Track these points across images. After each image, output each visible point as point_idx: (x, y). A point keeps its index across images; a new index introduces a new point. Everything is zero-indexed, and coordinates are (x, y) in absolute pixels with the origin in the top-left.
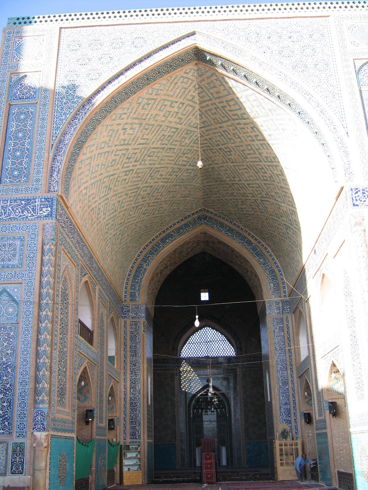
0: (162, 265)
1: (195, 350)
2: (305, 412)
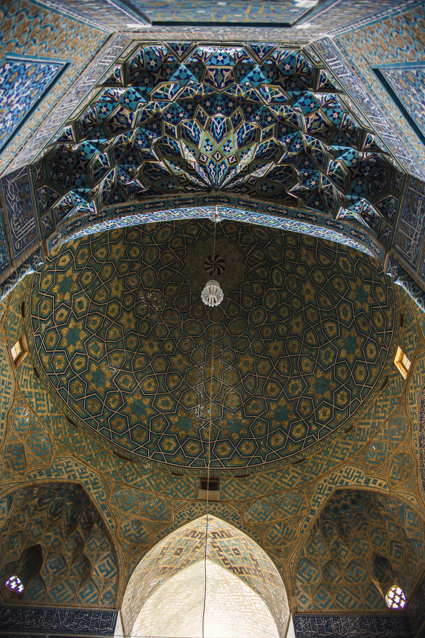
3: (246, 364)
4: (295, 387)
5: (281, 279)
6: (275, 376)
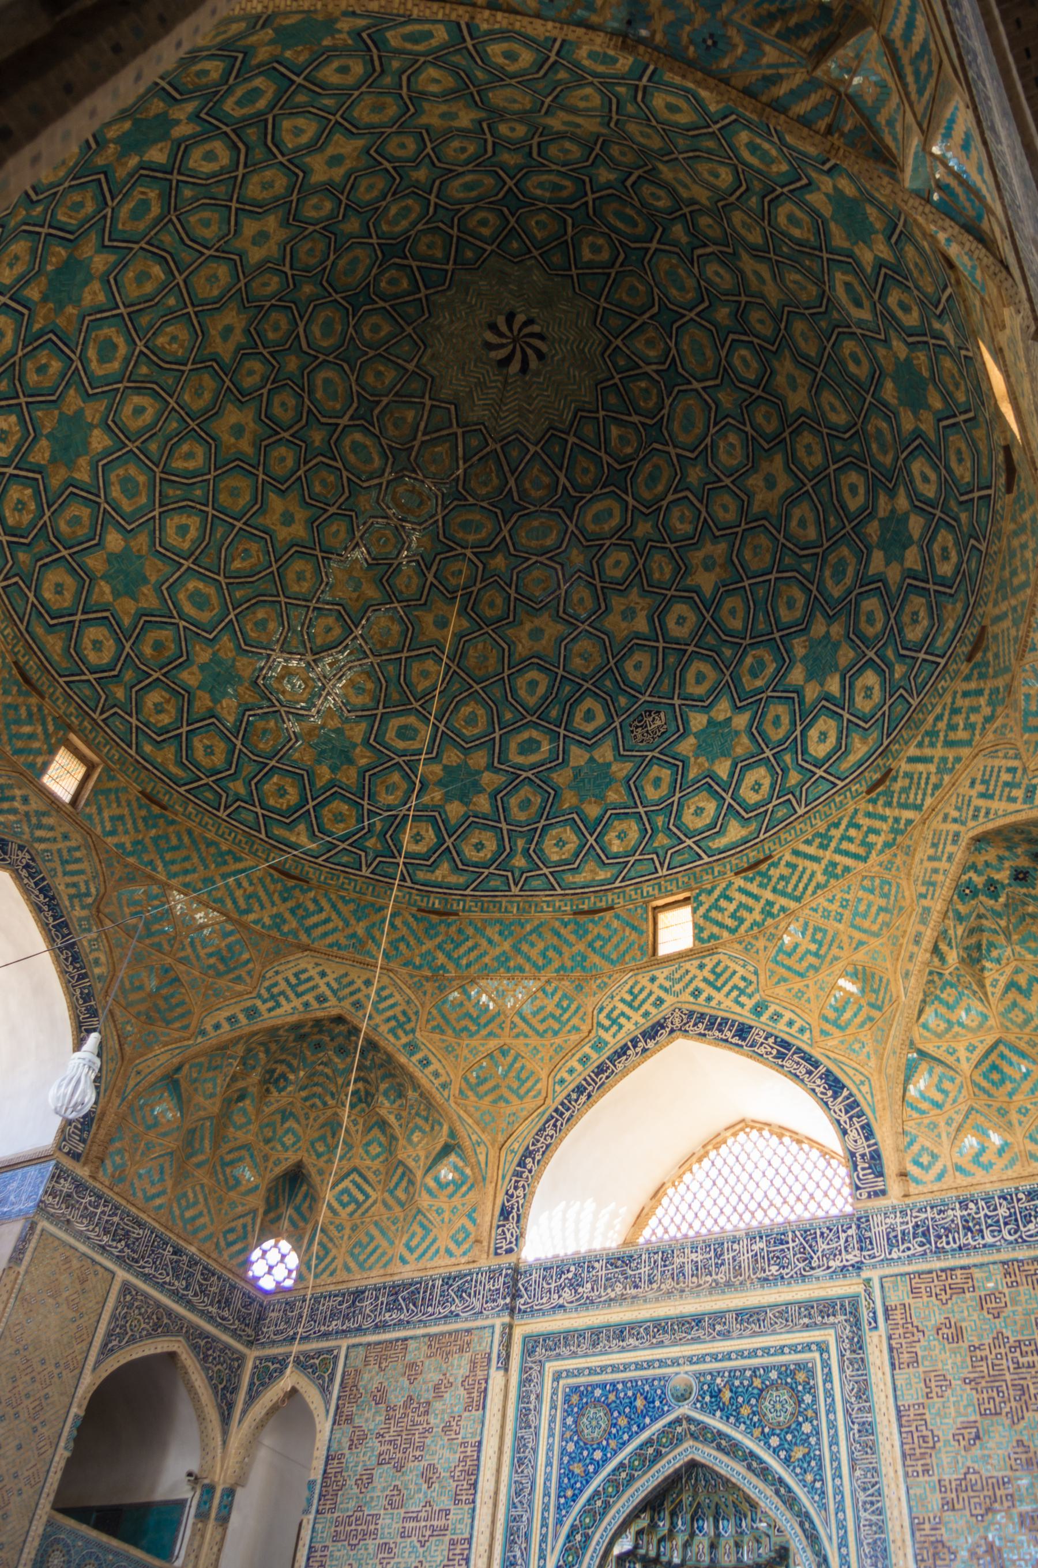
3: (262, 237)
4: (107, 349)
5: (352, 458)
6: (172, 301)
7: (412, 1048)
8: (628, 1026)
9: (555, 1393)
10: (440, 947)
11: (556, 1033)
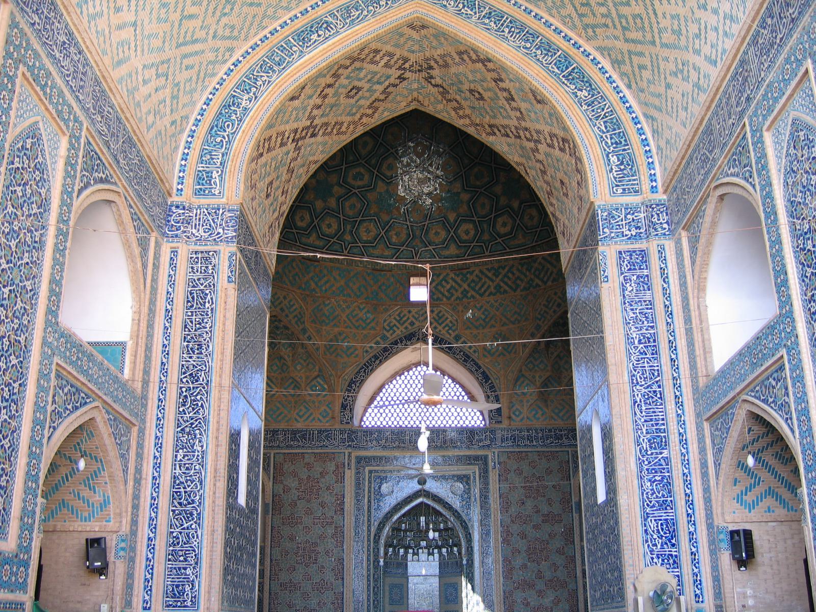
0: (296, 109)
1: (395, 415)
2: (732, 527)
7: (304, 331)
8: (398, 332)
9: (370, 477)
10: (312, 279)
11: (363, 329)
